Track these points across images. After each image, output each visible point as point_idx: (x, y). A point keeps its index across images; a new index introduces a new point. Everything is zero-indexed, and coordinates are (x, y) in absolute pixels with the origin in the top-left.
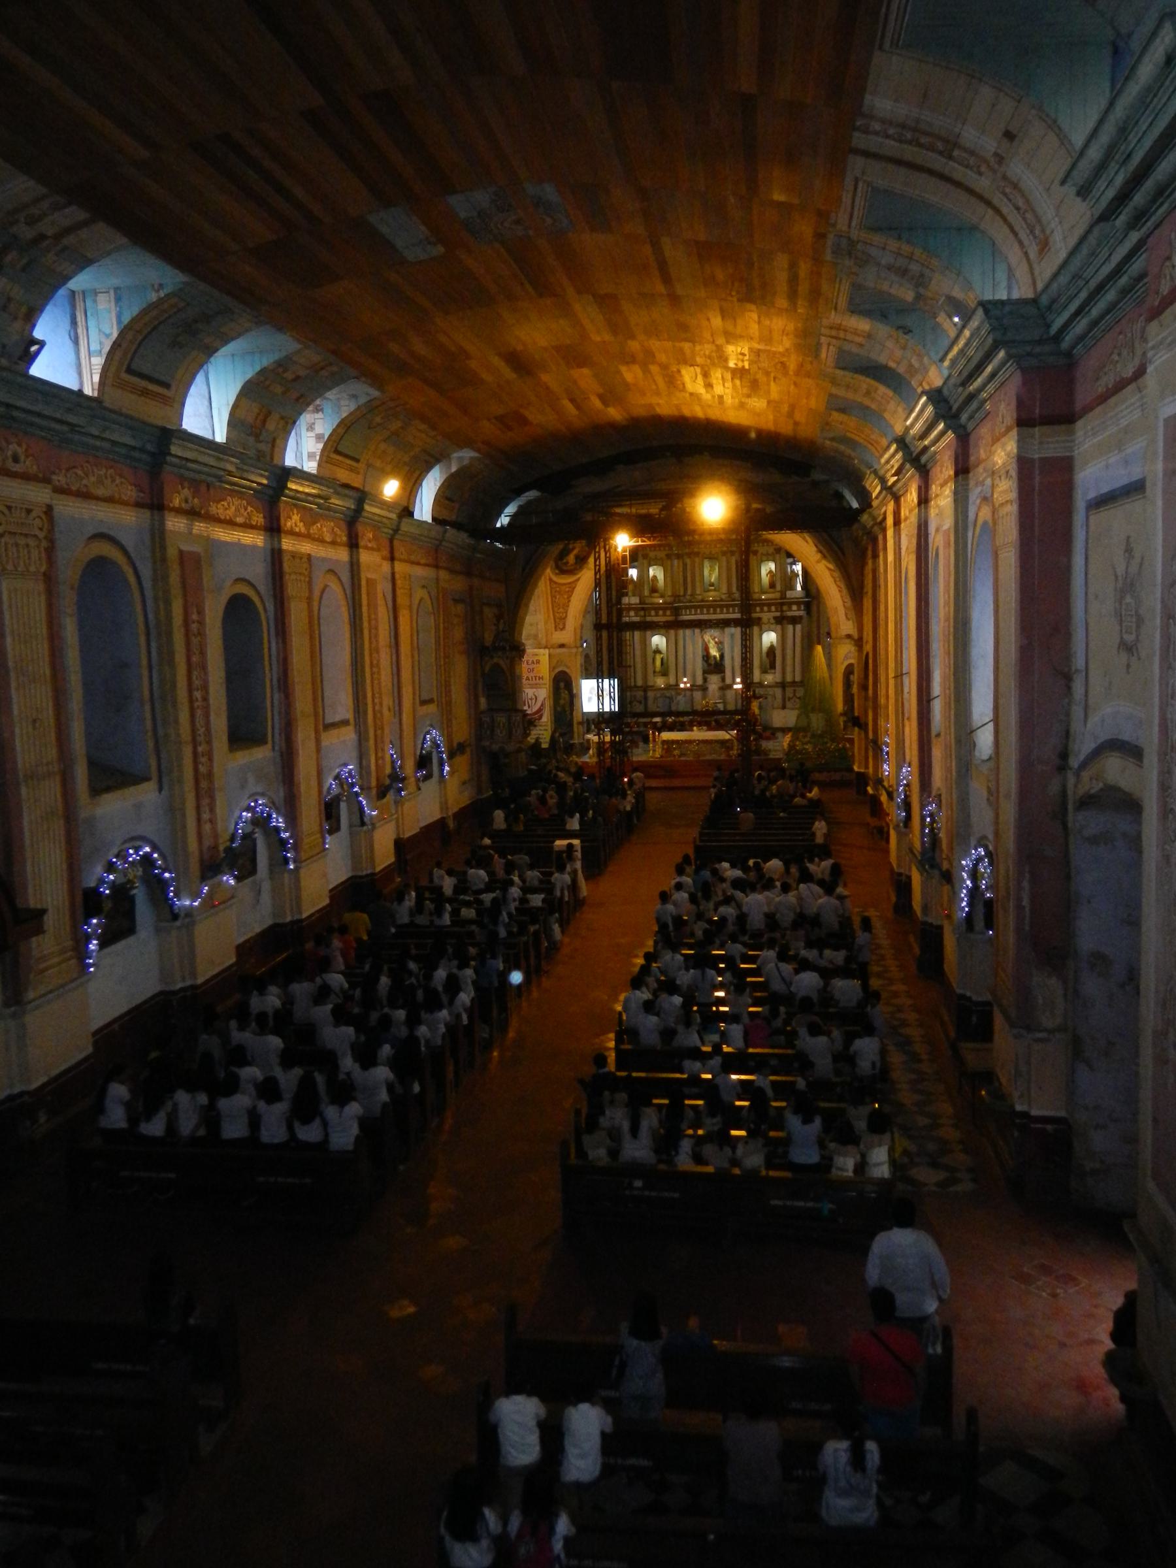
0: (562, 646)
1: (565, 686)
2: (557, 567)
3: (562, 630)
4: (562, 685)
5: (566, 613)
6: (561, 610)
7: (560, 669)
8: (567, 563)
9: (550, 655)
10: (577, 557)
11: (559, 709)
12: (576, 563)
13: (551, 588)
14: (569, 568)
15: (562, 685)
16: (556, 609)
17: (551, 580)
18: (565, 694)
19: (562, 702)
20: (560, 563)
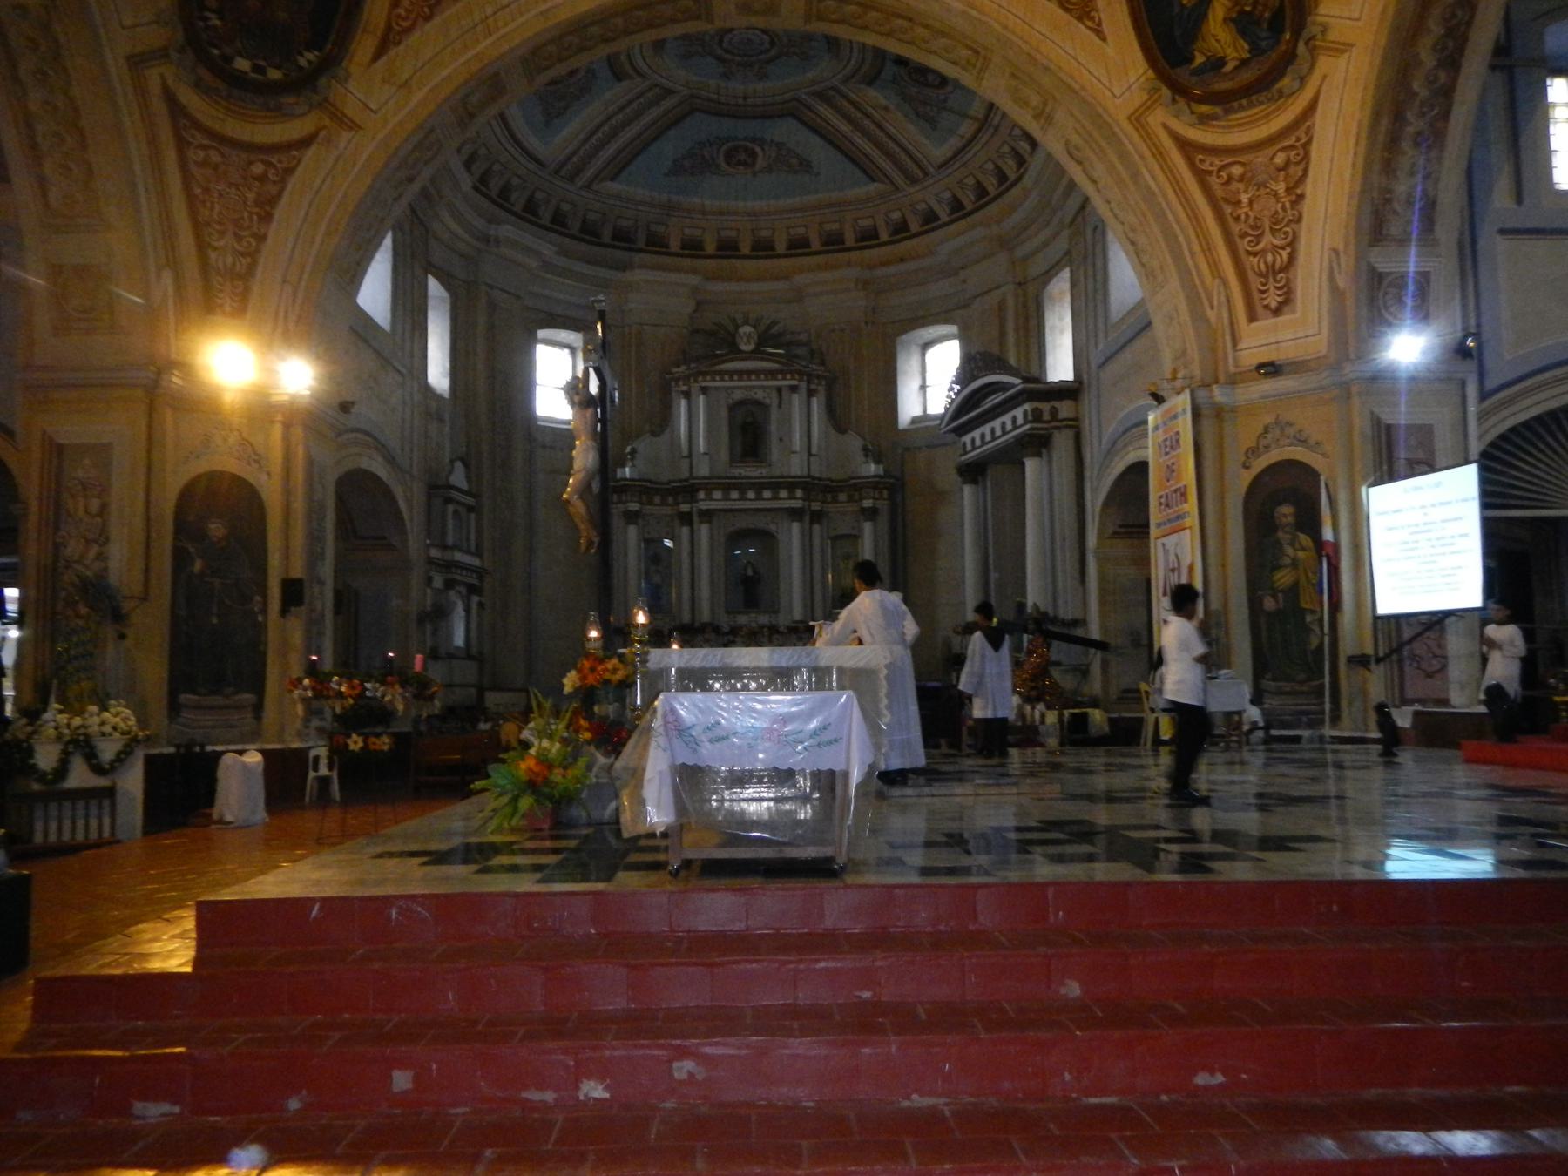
0: (1271, 369)
1: (1297, 515)
2: (1179, 90)
3: (1277, 312)
4: (1286, 512)
5: (1293, 243)
6: (1268, 239)
7: (1274, 456)
8: (1217, 64)
9: (1196, 415)
10: (1242, 23)
11: (1269, 604)
12: (1256, 51)
13: (1201, 176)
14: (1248, 76)
15: (1286, 512)
16: (1244, 245)
17: (1185, 146)
18: (1296, 549)
19: (1283, 578)
20: (1182, 74)
